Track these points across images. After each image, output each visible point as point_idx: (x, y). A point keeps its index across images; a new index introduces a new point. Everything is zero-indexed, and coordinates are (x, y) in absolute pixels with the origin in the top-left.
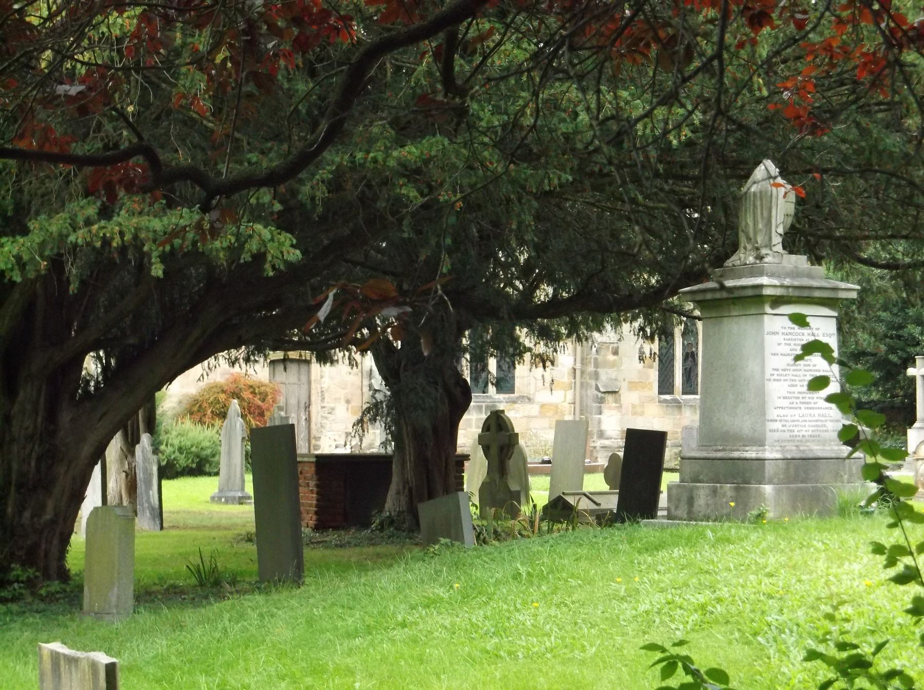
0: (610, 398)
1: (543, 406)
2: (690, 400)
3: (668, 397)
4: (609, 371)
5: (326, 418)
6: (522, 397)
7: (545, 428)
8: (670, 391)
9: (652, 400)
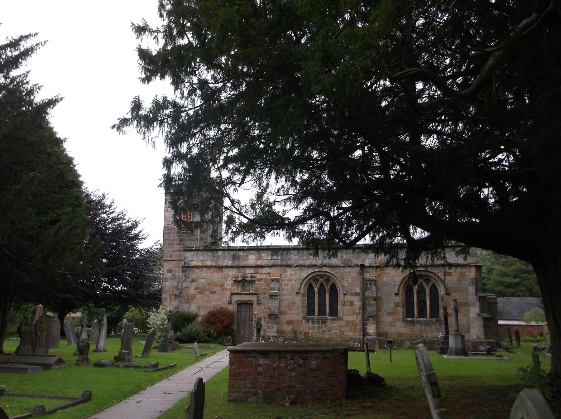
0: (371, 319)
1: (347, 322)
2: (421, 320)
3: (410, 319)
4: (372, 308)
7: (348, 331)
8: (413, 316)
9: (399, 320)
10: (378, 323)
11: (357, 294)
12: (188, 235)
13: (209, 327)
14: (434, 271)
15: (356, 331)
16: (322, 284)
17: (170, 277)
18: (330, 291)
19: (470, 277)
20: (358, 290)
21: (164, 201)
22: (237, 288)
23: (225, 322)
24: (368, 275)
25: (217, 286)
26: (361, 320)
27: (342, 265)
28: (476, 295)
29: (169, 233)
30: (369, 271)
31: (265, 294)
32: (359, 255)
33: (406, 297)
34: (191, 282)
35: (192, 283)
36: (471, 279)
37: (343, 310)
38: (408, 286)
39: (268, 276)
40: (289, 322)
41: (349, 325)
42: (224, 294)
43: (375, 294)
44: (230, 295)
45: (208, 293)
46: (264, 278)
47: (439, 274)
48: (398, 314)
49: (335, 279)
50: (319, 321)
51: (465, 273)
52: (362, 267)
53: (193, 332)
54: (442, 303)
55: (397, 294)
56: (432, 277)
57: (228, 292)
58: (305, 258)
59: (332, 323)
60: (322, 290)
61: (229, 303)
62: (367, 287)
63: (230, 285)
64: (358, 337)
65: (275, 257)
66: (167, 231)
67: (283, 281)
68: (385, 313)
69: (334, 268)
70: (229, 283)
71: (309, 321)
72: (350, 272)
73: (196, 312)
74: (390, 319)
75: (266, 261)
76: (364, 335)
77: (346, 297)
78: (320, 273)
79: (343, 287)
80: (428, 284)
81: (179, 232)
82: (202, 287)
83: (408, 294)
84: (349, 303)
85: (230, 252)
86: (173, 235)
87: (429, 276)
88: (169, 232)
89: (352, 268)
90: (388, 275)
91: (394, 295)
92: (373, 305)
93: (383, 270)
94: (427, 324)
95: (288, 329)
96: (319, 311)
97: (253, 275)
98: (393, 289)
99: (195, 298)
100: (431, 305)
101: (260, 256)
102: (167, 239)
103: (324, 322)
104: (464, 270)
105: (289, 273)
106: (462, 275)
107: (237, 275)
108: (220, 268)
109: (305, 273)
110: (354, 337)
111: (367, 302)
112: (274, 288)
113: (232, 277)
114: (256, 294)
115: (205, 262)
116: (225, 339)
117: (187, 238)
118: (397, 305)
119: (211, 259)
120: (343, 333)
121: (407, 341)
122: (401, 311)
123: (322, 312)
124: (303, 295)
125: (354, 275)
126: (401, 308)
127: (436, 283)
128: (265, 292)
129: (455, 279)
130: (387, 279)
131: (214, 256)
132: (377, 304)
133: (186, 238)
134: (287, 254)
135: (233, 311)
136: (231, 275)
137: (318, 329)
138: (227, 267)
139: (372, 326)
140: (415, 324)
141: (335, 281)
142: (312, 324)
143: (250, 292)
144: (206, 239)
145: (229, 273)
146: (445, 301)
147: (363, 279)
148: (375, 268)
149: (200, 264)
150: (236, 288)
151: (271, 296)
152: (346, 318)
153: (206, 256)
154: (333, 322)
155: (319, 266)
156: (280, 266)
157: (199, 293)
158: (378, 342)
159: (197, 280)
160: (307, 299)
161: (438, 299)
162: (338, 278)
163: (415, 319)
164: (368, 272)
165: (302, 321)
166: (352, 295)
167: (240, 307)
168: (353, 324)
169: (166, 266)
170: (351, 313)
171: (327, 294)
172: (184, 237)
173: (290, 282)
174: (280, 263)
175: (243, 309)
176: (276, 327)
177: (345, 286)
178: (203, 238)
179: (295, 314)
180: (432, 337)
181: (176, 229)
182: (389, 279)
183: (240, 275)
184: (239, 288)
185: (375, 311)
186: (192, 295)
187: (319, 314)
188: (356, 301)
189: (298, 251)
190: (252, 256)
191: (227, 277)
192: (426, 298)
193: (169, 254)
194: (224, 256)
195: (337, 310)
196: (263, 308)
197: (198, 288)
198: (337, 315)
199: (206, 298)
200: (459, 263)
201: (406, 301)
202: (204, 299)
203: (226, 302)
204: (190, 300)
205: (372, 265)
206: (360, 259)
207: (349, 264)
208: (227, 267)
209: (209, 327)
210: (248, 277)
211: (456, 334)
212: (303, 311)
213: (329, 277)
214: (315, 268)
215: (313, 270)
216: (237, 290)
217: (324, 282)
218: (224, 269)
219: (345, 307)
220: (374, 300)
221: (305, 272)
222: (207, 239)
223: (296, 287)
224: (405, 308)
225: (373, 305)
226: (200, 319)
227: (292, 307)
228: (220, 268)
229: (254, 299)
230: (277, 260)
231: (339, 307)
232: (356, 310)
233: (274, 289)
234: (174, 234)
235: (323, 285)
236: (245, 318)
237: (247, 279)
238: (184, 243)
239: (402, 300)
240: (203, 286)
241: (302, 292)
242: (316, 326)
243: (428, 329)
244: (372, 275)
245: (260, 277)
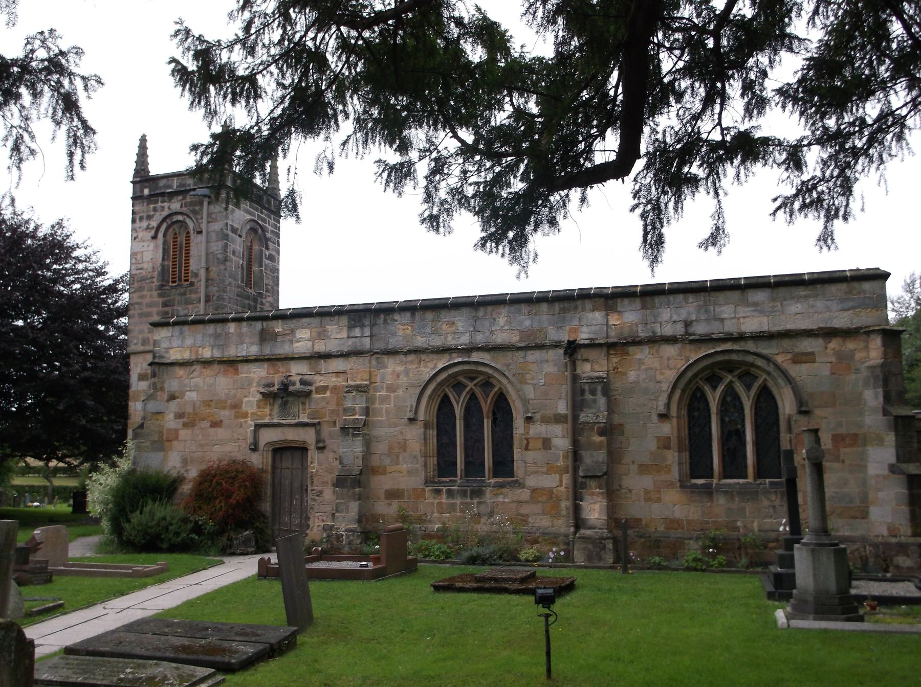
0: (593, 483)
1: (534, 490)
3: (700, 481)
4: (595, 453)
5: (315, 500)
6: (517, 481)
7: (538, 514)
9: (671, 485)
10: (612, 494)
11: (558, 419)
12: (182, 290)
13: (200, 508)
14: (765, 352)
15: (557, 515)
16: (473, 397)
17: (144, 391)
18: (494, 414)
19: (867, 364)
20: (562, 407)
21: (131, 216)
22: (271, 410)
23: (235, 495)
24: (587, 367)
25: (224, 408)
26: (571, 487)
27: (519, 345)
28: (885, 413)
29: (141, 289)
30: (591, 358)
31: (335, 423)
32: (564, 317)
33: (689, 423)
34: (168, 401)
35: (171, 402)
36: (872, 368)
37: (525, 462)
38: (694, 394)
39: (340, 380)
40: (393, 495)
41: (540, 499)
42: (241, 426)
43: (603, 416)
44: (253, 428)
45: (206, 424)
46: (331, 384)
47: (779, 359)
48: (668, 469)
49: (505, 381)
50: (466, 491)
51: (853, 352)
52: (572, 348)
53: (154, 523)
54: (788, 436)
55: (664, 417)
56: (758, 367)
57: (250, 422)
58: (428, 331)
59: (496, 495)
60: (472, 409)
61: (252, 450)
62: (583, 400)
63: (255, 405)
64: (562, 530)
65: (357, 332)
66: (136, 285)
67: (376, 390)
68: (634, 468)
69: (500, 355)
70: (251, 400)
71: (438, 492)
72: (541, 362)
73: (179, 472)
74: (647, 482)
75: (337, 341)
76: (577, 527)
77: (531, 426)
78: (467, 367)
79: (525, 402)
80: (748, 387)
81: (163, 286)
82: (191, 411)
83: (696, 414)
84: (539, 444)
85: (253, 323)
86: (149, 293)
87: (753, 365)
88: (140, 287)
89: (545, 351)
90: (640, 367)
91: (655, 418)
92: (599, 447)
93: (628, 354)
94: (748, 494)
95: (387, 509)
96: (467, 463)
97: (305, 377)
98: (655, 402)
99: (177, 438)
100: (757, 444)
101: (319, 330)
102: (137, 303)
103: (477, 493)
104: (850, 345)
105: (390, 370)
106: (844, 361)
107: (270, 381)
108: (232, 363)
109: (429, 368)
110: (551, 530)
111: (582, 439)
112: (354, 409)
113: (258, 385)
114: (313, 425)
115: (197, 351)
116: (237, 539)
117: (179, 298)
118: (665, 444)
119: (213, 344)
120: (524, 519)
121: (692, 542)
122: (677, 459)
123: (474, 466)
124: (426, 426)
125: (550, 368)
126: (676, 454)
127: (770, 384)
128: (334, 418)
129: (825, 371)
130: (638, 376)
131: (217, 336)
132: (609, 444)
133: (177, 298)
134: (385, 321)
135: (261, 466)
136: (256, 380)
137: (462, 511)
138: (247, 361)
139: (595, 503)
140: (715, 495)
141: (505, 387)
142: (448, 498)
143: (301, 420)
144: (220, 298)
145: (252, 375)
146: (796, 430)
147: (575, 378)
148: (605, 349)
149: (187, 355)
150: (267, 410)
151: (344, 430)
152: (531, 482)
153: (199, 337)
154: (499, 492)
155: (463, 349)
156: (370, 353)
157: (185, 425)
158: (610, 546)
159: (183, 394)
160: (438, 435)
161: (778, 426)
162: (510, 377)
163: (715, 481)
164: (587, 360)
165: (423, 490)
166: (546, 420)
167: (281, 456)
168: (551, 497)
169: (136, 366)
170: (545, 469)
171: (485, 421)
172: (172, 298)
173: (394, 391)
174: (368, 346)
175: (287, 462)
176: (354, 507)
177: (529, 400)
178: (214, 295)
180: (759, 531)
181: (155, 280)
182: (643, 376)
183: (277, 379)
184: (276, 409)
185: (603, 463)
186: (169, 430)
187: (467, 473)
188: (557, 437)
189: (413, 315)
190: (304, 331)
191: (248, 386)
192: (744, 426)
193: (141, 336)
194: (240, 335)
195: (512, 461)
196: (331, 460)
197: (184, 413)
198: (511, 473)
199: (200, 437)
200: (837, 326)
201: (689, 434)
202: (196, 441)
203: (245, 446)
204: (166, 443)
205: (597, 342)
206: (567, 328)
207: (537, 341)
208: (247, 361)
209: (200, 508)
210: (294, 384)
211: (816, 544)
212: (425, 465)
213: (489, 377)
214: (454, 355)
216: (270, 415)
217: (478, 392)
218: (240, 366)
220: (601, 433)
221: (431, 365)
222: (223, 299)
223: (408, 404)
224: (687, 453)
225: (599, 447)
226: (186, 488)
227: (398, 457)
228: (232, 363)
229: (308, 436)
230: (362, 338)
231: (517, 453)
232: (557, 461)
233: (352, 411)
234: (151, 290)
235: (476, 398)
236: (291, 484)
237: (291, 388)
238: (173, 310)
239: (679, 430)
240: (194, 410)
241: (421, 416)
242: (458, 502)
243: (749, 507)
244: (596, 367)
245: (321, 384)
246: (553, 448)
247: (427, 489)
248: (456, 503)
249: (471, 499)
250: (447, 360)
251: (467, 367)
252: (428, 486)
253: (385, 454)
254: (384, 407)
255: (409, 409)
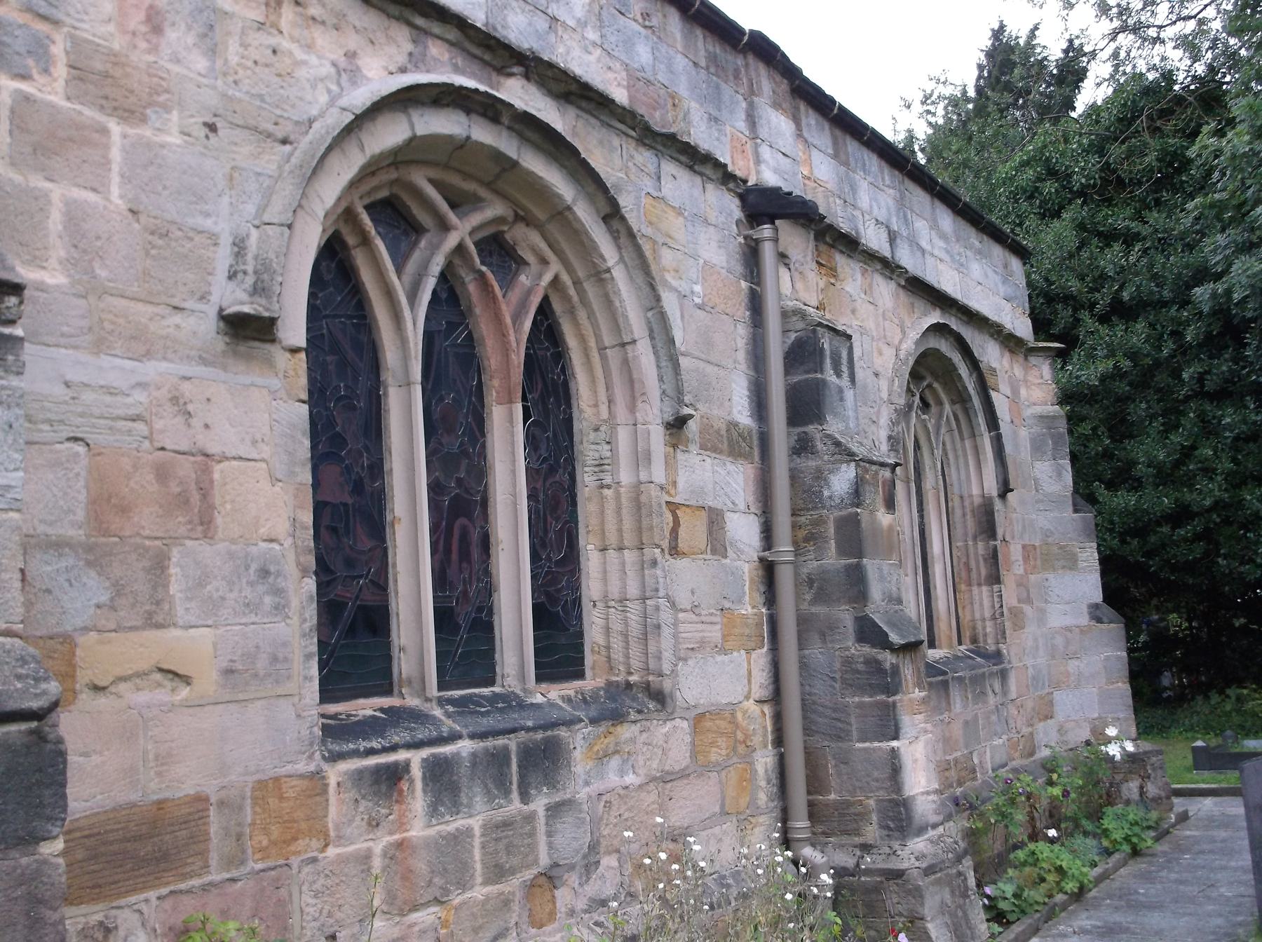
71: (392, 777)
77: (680, 456)
170: (715, 634)
173: (131, 114)
179: (208, 681)
215: (415, 61)
219: (681, 564)
223: (224, 229)
227: (159, 565)
242: (476, 823)
246: (730, 552)
247: (335, 773)
248: (468, 832)
249: (525, 797)
250: (402, 59)
251: (483, 134)
252: (335, 757)
253: (57, 546)
254: (57, 192)
255: (223, 258)
